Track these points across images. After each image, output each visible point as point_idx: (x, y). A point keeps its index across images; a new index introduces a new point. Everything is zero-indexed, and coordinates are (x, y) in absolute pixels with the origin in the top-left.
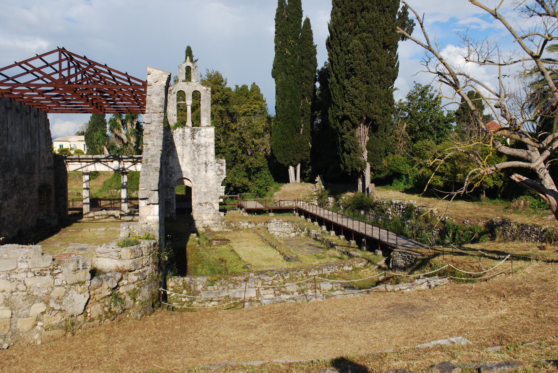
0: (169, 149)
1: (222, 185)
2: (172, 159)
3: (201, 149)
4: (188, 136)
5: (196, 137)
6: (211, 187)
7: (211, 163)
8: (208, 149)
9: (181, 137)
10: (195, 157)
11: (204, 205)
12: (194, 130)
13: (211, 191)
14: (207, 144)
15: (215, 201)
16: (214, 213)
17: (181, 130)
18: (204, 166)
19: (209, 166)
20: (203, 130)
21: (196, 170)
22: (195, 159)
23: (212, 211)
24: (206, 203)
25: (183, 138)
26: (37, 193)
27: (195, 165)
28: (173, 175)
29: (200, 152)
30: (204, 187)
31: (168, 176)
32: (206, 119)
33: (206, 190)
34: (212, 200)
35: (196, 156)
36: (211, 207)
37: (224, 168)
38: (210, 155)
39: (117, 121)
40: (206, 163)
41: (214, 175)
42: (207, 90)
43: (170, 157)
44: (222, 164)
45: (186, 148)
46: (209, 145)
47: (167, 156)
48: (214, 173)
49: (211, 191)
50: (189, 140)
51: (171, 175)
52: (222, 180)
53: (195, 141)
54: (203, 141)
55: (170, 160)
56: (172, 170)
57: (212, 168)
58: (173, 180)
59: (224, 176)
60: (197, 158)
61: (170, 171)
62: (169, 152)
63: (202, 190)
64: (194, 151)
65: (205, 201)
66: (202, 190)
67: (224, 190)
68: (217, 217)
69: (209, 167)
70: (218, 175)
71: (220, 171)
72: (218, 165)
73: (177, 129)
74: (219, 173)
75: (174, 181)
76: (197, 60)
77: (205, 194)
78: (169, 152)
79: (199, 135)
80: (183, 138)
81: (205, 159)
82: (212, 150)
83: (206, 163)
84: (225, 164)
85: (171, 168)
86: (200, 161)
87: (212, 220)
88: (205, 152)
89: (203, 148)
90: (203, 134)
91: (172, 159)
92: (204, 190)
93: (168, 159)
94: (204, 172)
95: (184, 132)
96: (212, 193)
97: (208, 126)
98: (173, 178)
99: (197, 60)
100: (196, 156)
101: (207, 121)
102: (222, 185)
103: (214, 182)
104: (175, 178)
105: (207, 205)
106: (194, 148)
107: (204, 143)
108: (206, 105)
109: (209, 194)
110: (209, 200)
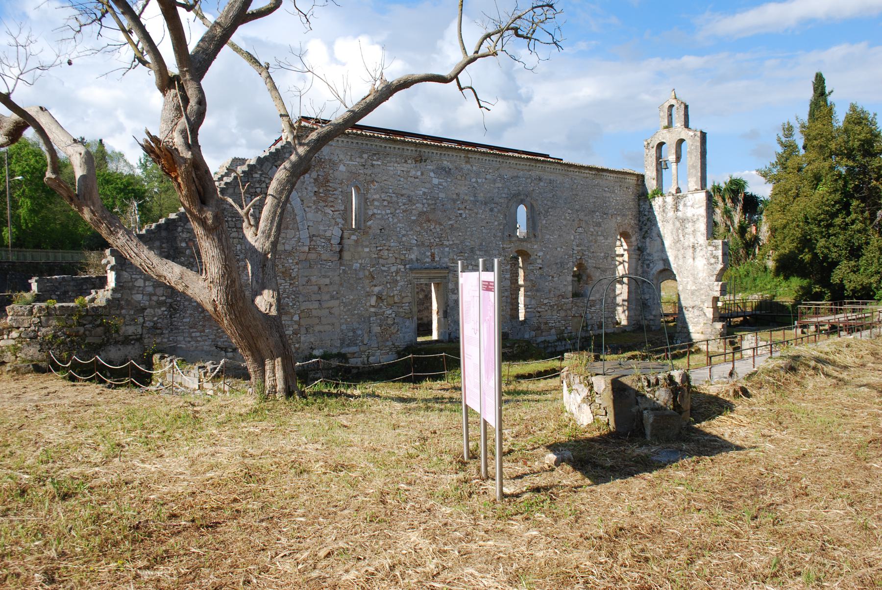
0: (646, 227)
1: (717, 280)
2: (650, 243)
3: (687, 226)
4: (669, 207)
5: (681, 207)
6: (701, 283)
7: (701, 246)
8: (697, 226)
9: (661, 209)
10: (679, 238)
11: (690, 309)
12: (678, 197)
13: (701, 289)
14: (696, 217)
15: (706, 305)
16: (705, 324)
17: (661, 199)
18: (691, 250)
19: (698, 250)
20: (690, 196)
21: (680, 256)
22: (679, 241)
23: (702, 320)
24: (693, 307)
25: (664, 211)
26: (627, 294)
27: (678, 250)
28: (651, 265)
29: (686, 231)
30: (690, 283)
31: (645, 266)
32: (694, 179)
33: (694, 288)
34: (703, 302)
35: (681, 236)
36: (701, 313)
37: (719, 253)
38: (699, 234)
39: (716, 198)
40: (693, 247)
41: (705, 265)
42: (695, 135)
43: (648, 240)
44: (716, 247)
45: (667, 224)
46: (698, 219)
47: (644, 238)
48: (705, 262)
49: (701, 289)
50: (671, 214)
51: (648, 265)
52: (716, 272)
53: (679, 214)
54: (689, 212)
55: (647, 244)
56: (650, 258)
57: (701, 253)
58: (652, 272)
59: (720, 266)
60: (682, 239)
61: (648, 260)
62: (647, 232)
63: (689, 288)
64: (678, 229)
65: (692, 304)
66: (689, 288)
67: (718, 288)
68: (710, 330)
69: (699, 253)
70: (711, 264)
71: (714, 257)
72: (710, 248)
73: (656, 198)
74: (713, 261)
75: (653, 274)
76: (832, 91)
77: (693, 293)
78: (647, 232)
79: (685, 205)
80: (664, 211)
81: (692, 240)
82: (702, 226)
83: (693, 247)
84: (721, 247)
85: (649, 255)
86: (687, 244)
87: (702, 333)
88: (693, 229)
89: (690, 224)
90: (689, 204)
91: (650, 243)
92: (691, 287)
93: (645, 243)
94: (691, 260)
95: (665, 202)
96: (702, 292)
97: (697, 190)
98: (652, 269)
99: (832, 91)
100: (681, 236)
101: (696, 182)
102: (717, 280)
103: (705, 275)
104: (654, 270)
105: (695, 310)
106: (678, 224)
107: (691, 215)
108: (694, 158)
109: (698, 294)
110: (698, 303)
